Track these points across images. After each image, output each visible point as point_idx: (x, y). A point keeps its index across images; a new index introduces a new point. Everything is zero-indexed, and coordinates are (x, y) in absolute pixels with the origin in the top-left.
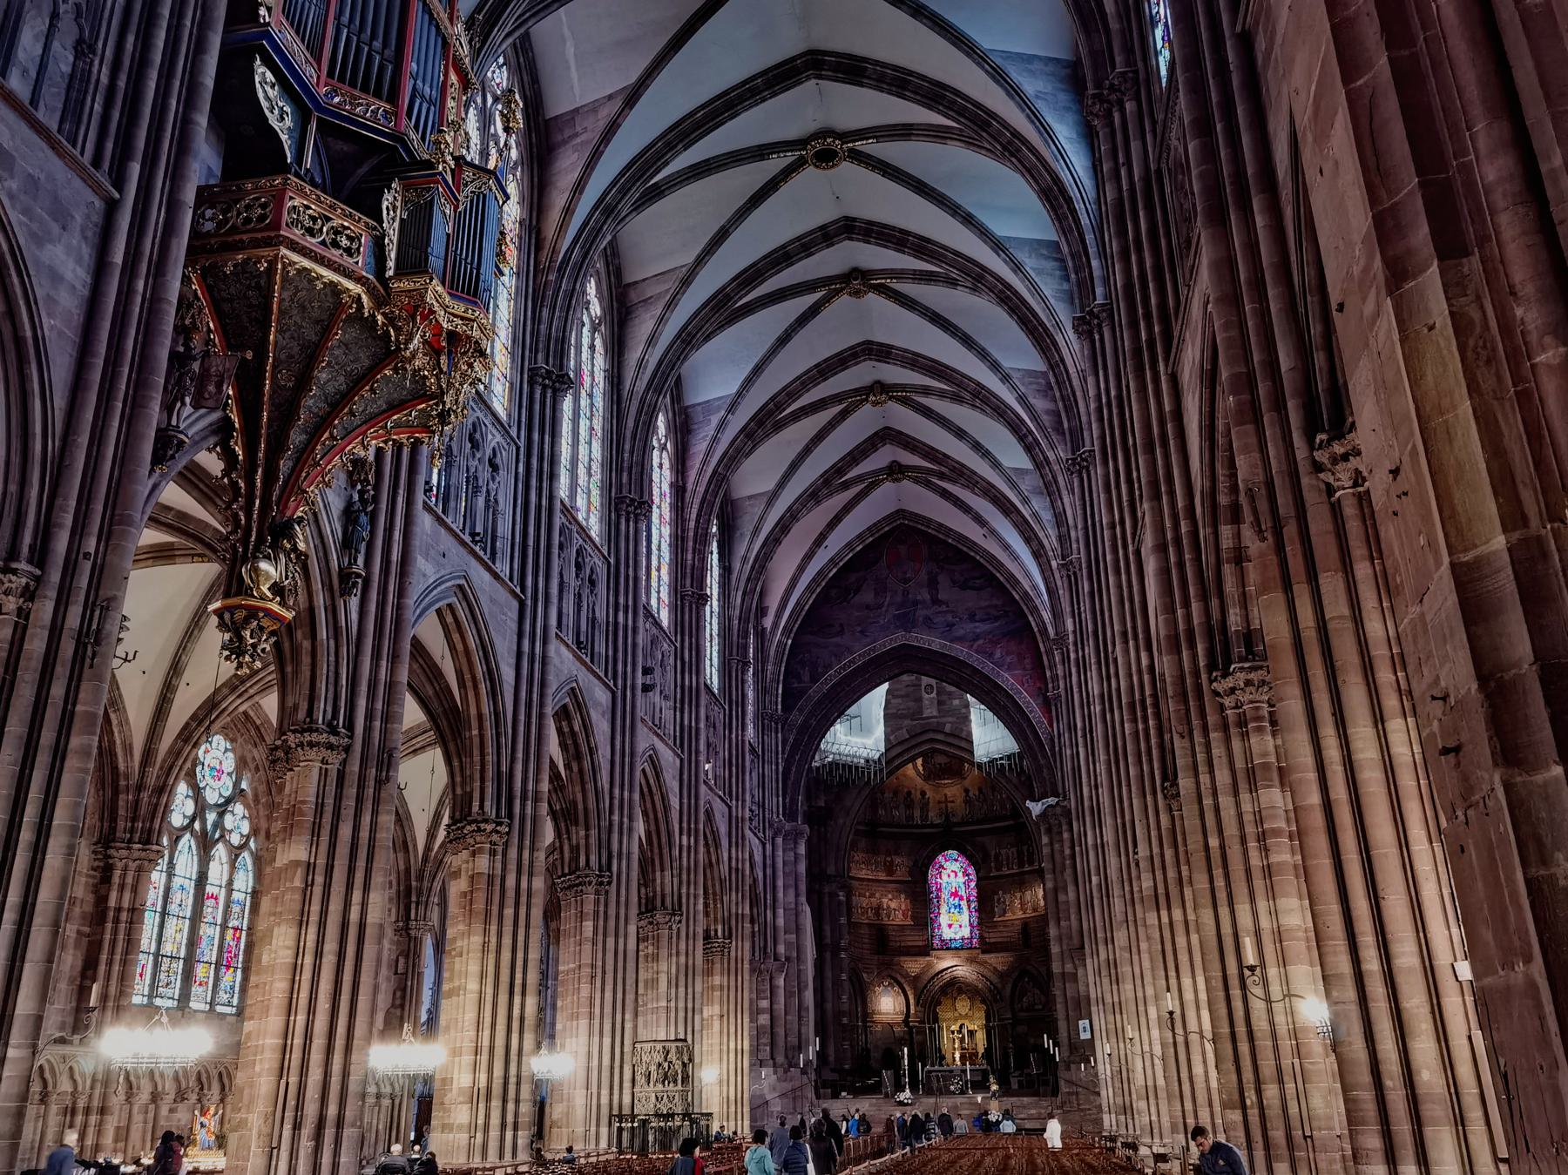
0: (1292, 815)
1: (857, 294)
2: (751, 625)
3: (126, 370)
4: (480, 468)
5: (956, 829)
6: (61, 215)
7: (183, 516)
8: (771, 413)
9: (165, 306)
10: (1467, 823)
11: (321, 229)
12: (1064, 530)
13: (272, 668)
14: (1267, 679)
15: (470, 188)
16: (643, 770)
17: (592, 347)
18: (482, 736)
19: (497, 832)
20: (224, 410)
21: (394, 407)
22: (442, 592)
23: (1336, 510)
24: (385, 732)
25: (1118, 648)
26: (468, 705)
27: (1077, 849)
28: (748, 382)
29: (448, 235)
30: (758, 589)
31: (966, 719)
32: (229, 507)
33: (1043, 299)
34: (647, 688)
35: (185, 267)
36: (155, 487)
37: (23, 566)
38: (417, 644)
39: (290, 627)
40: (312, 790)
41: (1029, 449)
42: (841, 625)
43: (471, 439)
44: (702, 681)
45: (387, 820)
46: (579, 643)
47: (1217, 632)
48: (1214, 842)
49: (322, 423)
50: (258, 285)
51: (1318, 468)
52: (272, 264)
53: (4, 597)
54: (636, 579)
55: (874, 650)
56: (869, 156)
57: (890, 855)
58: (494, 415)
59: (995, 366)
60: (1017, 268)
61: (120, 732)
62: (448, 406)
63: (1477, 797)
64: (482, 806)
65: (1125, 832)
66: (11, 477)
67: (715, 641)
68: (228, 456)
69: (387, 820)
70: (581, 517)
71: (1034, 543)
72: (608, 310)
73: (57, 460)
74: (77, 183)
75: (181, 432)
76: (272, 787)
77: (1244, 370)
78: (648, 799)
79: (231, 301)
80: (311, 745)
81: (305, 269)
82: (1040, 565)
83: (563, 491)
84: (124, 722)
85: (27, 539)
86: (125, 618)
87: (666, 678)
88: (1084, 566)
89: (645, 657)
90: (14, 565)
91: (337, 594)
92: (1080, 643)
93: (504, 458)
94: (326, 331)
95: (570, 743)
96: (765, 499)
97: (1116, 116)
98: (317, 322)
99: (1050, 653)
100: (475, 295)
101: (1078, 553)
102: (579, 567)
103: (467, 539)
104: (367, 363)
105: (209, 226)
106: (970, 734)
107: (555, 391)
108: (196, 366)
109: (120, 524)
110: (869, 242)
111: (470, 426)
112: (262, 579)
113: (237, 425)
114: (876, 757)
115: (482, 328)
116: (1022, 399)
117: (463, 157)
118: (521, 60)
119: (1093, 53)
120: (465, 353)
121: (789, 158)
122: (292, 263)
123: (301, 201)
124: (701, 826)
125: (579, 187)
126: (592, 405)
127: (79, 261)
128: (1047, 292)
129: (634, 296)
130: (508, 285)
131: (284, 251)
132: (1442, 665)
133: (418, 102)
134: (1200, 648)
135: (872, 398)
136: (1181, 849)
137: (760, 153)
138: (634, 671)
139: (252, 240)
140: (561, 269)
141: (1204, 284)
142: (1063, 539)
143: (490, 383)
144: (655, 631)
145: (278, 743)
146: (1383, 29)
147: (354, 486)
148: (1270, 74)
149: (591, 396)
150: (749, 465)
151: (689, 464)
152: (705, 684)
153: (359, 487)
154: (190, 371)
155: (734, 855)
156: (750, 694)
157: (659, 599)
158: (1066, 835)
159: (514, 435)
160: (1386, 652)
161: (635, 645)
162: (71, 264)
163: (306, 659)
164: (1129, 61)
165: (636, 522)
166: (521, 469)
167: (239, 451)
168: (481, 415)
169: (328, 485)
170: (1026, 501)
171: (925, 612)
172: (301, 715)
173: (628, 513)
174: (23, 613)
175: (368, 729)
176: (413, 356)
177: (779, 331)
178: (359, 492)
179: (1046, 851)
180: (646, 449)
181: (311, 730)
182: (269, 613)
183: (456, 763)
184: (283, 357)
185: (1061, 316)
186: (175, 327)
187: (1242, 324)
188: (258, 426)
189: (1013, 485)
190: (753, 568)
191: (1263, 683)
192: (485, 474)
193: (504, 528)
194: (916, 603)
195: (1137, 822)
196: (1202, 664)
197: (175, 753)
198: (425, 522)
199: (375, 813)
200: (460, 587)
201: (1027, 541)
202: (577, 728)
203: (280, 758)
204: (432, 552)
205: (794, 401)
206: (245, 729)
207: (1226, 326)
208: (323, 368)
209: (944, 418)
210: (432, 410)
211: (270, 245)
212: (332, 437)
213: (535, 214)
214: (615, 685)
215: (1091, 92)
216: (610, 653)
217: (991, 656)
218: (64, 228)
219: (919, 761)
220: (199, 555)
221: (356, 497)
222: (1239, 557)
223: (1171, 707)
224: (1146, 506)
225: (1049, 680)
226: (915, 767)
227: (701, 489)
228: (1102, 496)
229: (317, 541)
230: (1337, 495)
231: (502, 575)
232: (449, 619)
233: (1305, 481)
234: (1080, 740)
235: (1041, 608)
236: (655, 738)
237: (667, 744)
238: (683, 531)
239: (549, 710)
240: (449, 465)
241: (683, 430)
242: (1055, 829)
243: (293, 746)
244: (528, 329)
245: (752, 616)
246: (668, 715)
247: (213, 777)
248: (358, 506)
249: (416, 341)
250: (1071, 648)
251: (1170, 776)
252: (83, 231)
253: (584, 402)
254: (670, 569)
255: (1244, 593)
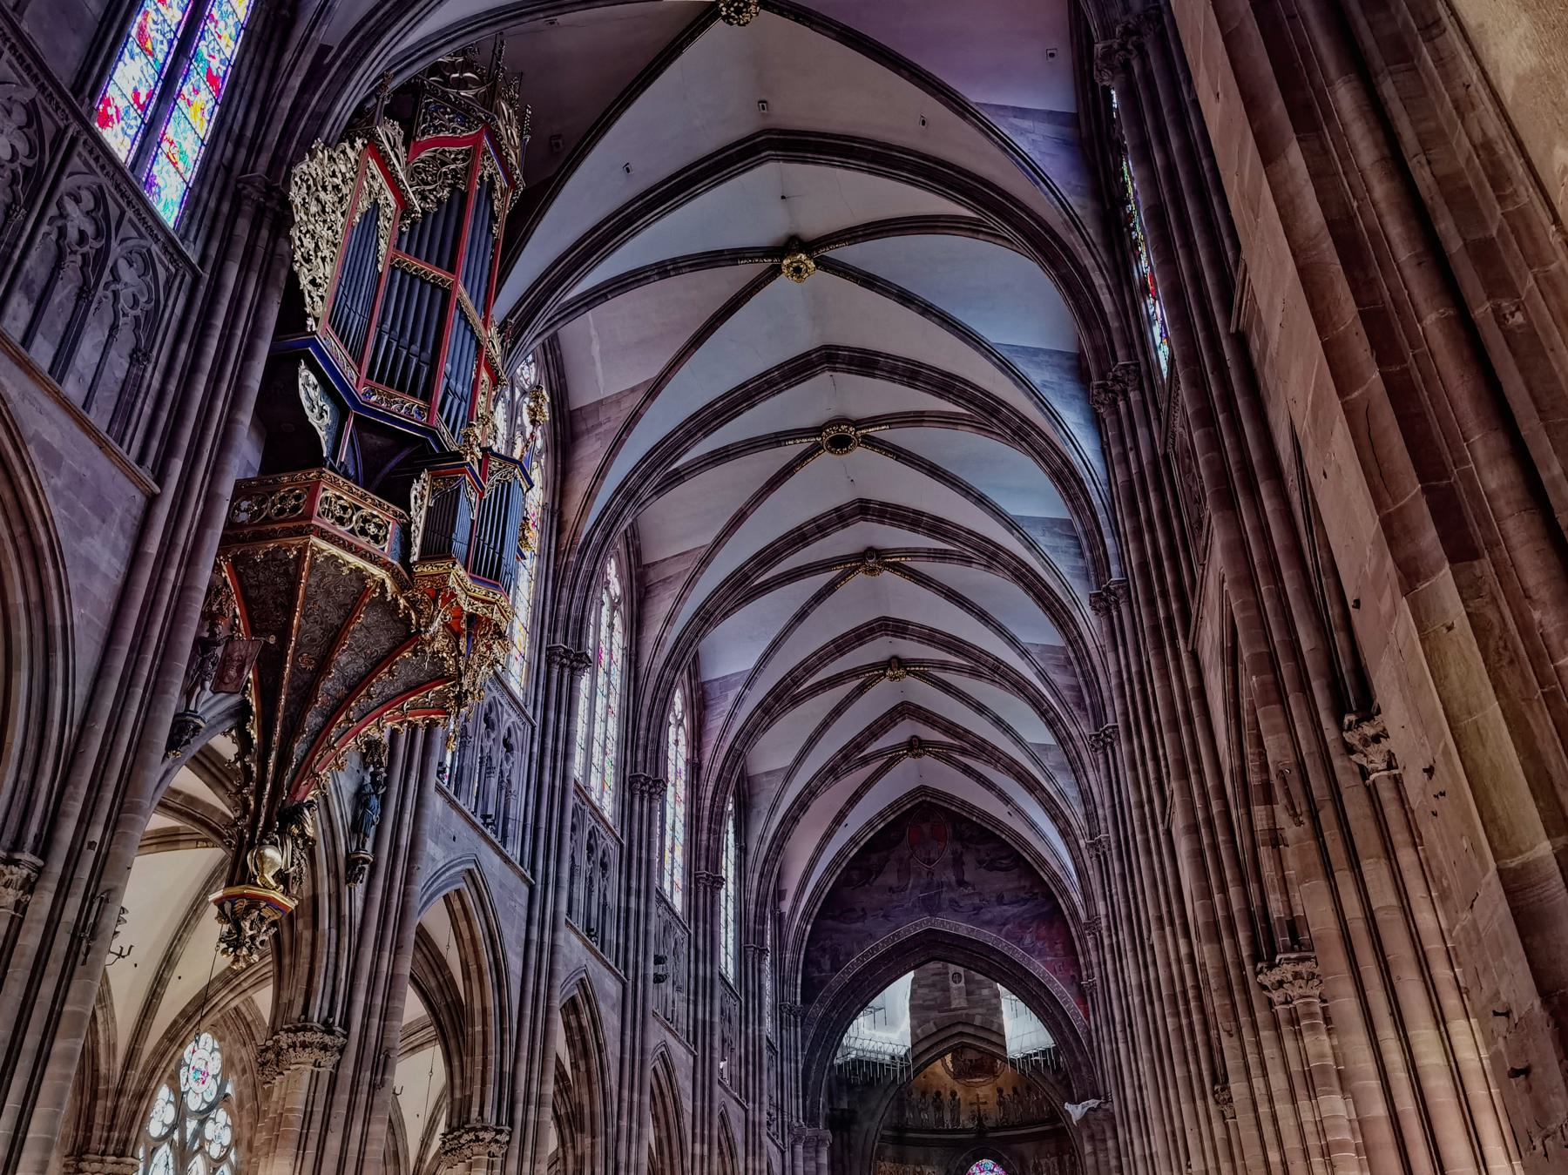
0: (1356, 1125)
1: (872, 571)
2: (768, 910)
3: (150, 657)
4: (495, 749)
5: (990, 1135)
6: (101, 508)
7: (192, 800)
8: (788, 688)
9: (194, 594)
10: (1546, 1155)
11: (351, 518)
12: (1090, 807)
13: (269, 959)
14: (1317, 971)
15: (496, 477)
16: (655, 1069)
17: (611, 626)
18: (485, 1033)
19: (497, 1141)
20: (243, 694)
21: (412, 688)
22: (451, 877)
23: (1372, 793)
24: (383, 1030)
25: (1154, 934)
26: (472, 999)
27: (1124, 1159)
28: (766, 658)
29: (473, 521)
30: (776, 871)
31: (997, 1010)
32: (239, 791)
33: (1059, 576)
34: (659, 979)
35: (218, 555)
36: (167, 772)
37: (26, 856)
38: (422, 933)
39: (291, 917)
40: (302, 1097)
41: (1051, 724)
42: (863, 910)
43: (487, 719)
44: (716, 971)
45: (379, 1129)
46: (589, 930)
47: (1258, 919)
48: (1274, 1157)
49: (340, 705)
50: (286, 572)
51: (1349, 749)
52: (301, 552)
53: (3, 889)
54: (649, 861)
55: (897, 935)
56: (882, 442)
57: (918, 1164)
58: (511, 695)
59: (1012, 641)
60: (1031, 545)
61: (104, 1031)
62: (465, 689)
63: (1554, 1126)
64: (481, 1113)
65: (1175, 1141)
66: (24, 766)
67: (731, 926)
68: (244, 740)
69: (379, 1129)
70: (594, 797)
71: (1061, 823)
72: (628, 589)
73: (72, 747)
74: (121, 478)
75: (198, 717)
76: (258, 1093)
77: (1264, 649)
78: (658, 1100)
79: (258, 587)
80: (304, 1045)
81: (333, 556)
82: (1067, 844)
83: (577, 770)
84: (110, 1019)
85: (33, 829)
86: (123, 910)
87: (678, 968)
88: (1113, 845)
89: (657, 947)
90: (17, 856)
91: (342, 881)
92: (1113, 927)
93: (520, 737)
94: (349, 614)
95: (580, 1043)
96: (783, 775)
97: (1121, 404)
98: (341, 606)
99: (1082, 938)
100: (497, 579)
101: (1107, 833)
102: (590, 849)
103: (479, 821)
104: (387, 645)
105: (244, 517)
106: (1001, 1026)
107: (573, 669)
108: (219, 651)
109: (130, 810)
110: (883, 523)
111: (486, 706)
112: (266, 866)
113: (254, 709)
114: (903, 1053)
115: (502, 611)
116: (1042, 674)
117: (490, 448)
118: (549, 357)
119: (1096, 350)
120: (485, 635)
121: (803, 445)
122: (321, 551)
123: (334, 492)
124: (715, 1133)
125: (601, 473)
126: (609, 683)
127: (114, 550)
128: (1063, 569)
129: (653, 576)
130: (528, 566)
131: (314, 539)
132: (1500, 977)
133: (450, 399)
134: (1242, 937)
135: (889, 673)
136: (1238, 1162)
137: (777, 439)
138: (645, 960)
139: (283, 529)
140: (582, 551)
141: (1217, 565)
142: (1091, 817)
143: (508, 662)
144: (667, 916)
145: (270, 1043)
146: (1372, 347)
147: (366, 769)
148: (1266, 369)
149: (608, 673)
150: (765, 741)
151: (705, 740)
152: (720, 974)
153: (371, 769)
154: (212, 656)
155: (750, 1166)
156: (768, 985)
157: (672, 882)
158: (1110, 1144)
159: (530, 714)
160: (1440, 945)
161: (646, 932)
162: (107, 555)
163: (305, 951)
164: (1131, 355)
165: (650, 802)
166: (535, 749)
167: (254, 734)
168: (497, 695)
169: (340, 768)
170: (1050, 778)
171: (952, 895)
172: (296, 1012)
173: (642, 792)
174: (22, 908)
175: (365, 1027)
176: (433, 639)
177: (796, 608)
178: (372, 774)
179: (1089, 1161)
180: (662, 726)
181: (304, 1029)
182: (271, 902)
183: (456, 1063)
184: (305, 641)
185: (1078, 593)
186: (203, 613)
187: (1259, 605)
188: (275, 709)
189: (1037, 762)
190: (770, 849)
191: (1312, 976)
192: (499, 754)
193: (516, 809)
194: (940, 885)
195: (1188, 1131)
196: (1245, 954)
197: (160, 1054)
198: (436, 804)
199: (367, 1122)
200: (470, 872)
201: (1054, 819)
202: (585, 1023)
203: (270, 1060)
204: (442, 836)
205: (811, 676)
206: (238, 1025)
207: (1244, 607)
208: (344, 651)
209: (963, 693)
210: (449, 691)
211: (301, 534)
212: (348, 720)
213: (557, 499)
214: (626, 976)
215: (1096, 382)
216: (621, 941)
217: (1019, 941)
218: (104, 521)
219: (948, 1058)
220: (205, 840)
221: (368, 779)
222: (1276, 840)
223: (1216, 1001)
224: (1174, 785)
225: (1083, 967)
226: (944, 1064)
227: (718, 766)
228: (1128, 774)
229: (326, 826)
230: (1372, 777)
231: (512, 859)
232: (457, 905)
233: (1338, 763)
234: (1120, 1035)
235: (1070, 890)
236: (667, 1033)
237: (680, 1041)
238: (698, 810)
239: (557, 1003)
240: (463, 745)
241: (700, 706)
242: (1098, 1137)
243: (285, 1046)
244: (548, 609)
245: (769, 899)
246: (681, 1007)
247: (197, 1080)
248: (369, 789)
249: (436, 624)
250: (1105, 933)
251: (1220, 1078)
252: (122, 523)
253: (601, 679)
254: (684, 850)
255: (1284, 877)
